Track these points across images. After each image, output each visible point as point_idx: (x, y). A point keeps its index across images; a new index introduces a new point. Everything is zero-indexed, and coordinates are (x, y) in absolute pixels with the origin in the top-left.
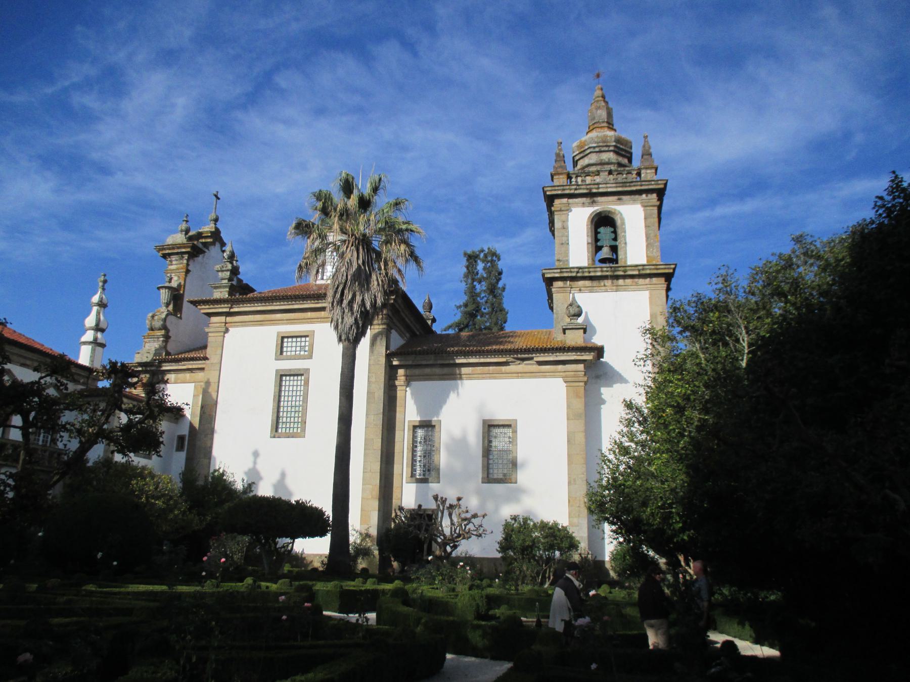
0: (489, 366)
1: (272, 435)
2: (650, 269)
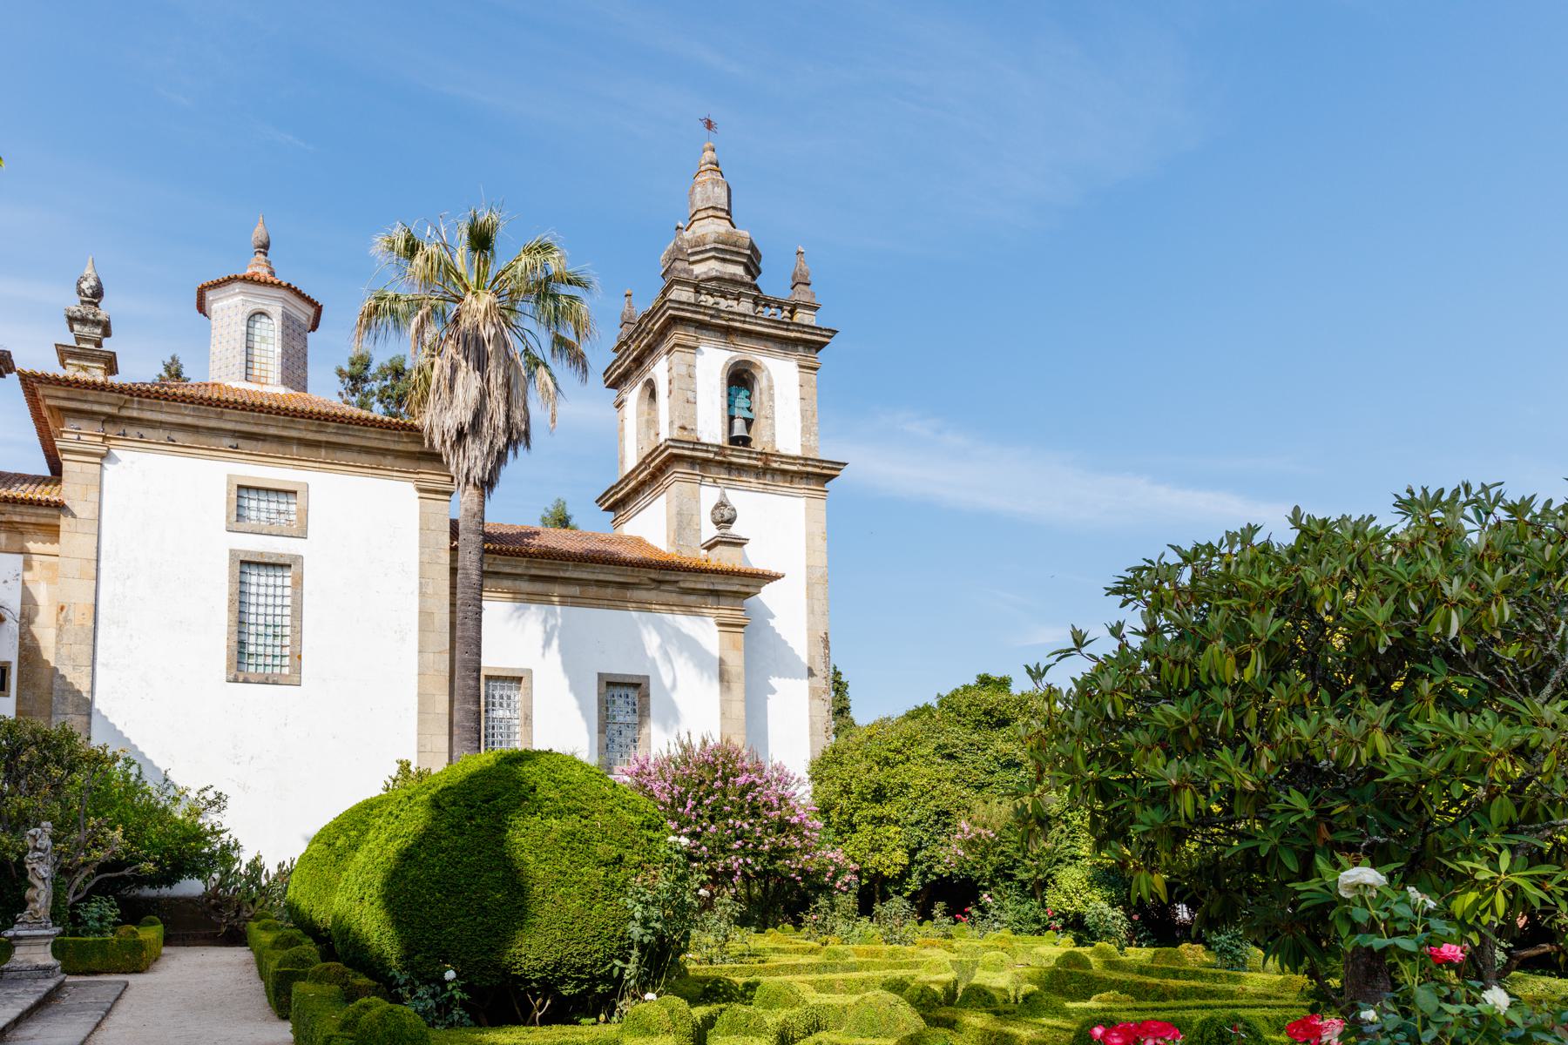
0: (607, 587)
1: (231, 677)
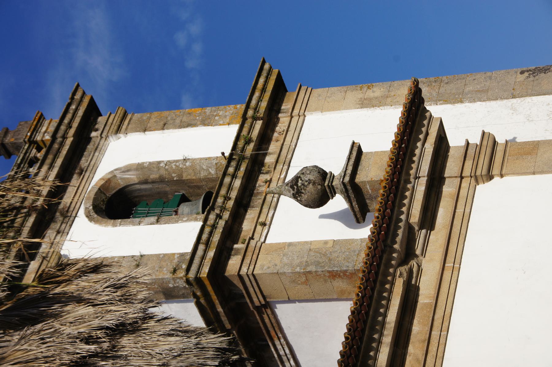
2: (260, 99)
